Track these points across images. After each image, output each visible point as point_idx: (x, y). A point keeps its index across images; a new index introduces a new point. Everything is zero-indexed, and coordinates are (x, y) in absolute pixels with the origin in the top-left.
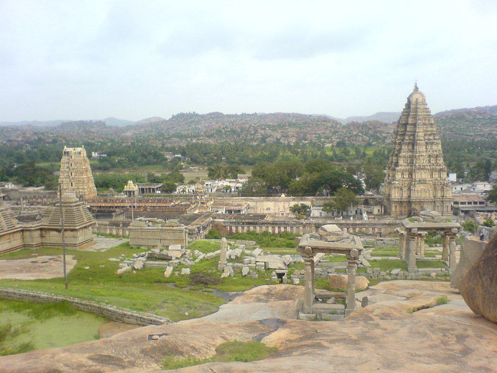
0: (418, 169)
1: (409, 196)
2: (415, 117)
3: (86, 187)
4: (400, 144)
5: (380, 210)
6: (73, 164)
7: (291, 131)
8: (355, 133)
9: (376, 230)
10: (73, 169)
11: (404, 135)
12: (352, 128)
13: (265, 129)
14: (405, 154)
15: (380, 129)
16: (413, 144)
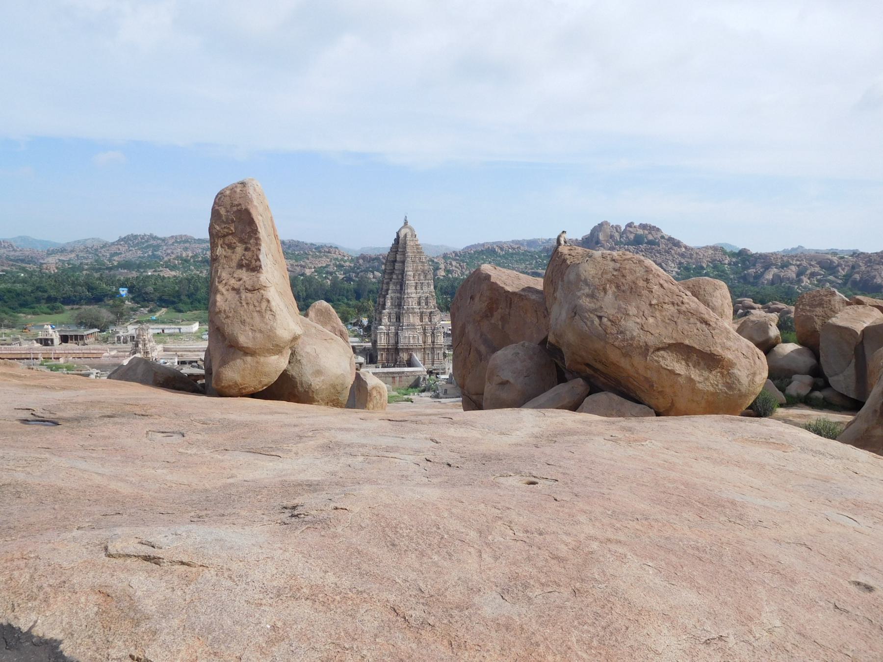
1: (397, 343)
2: (404, 253)
4: (388, 283)
11: (392, 273)
12: (361, 261)
16: (402, 285)
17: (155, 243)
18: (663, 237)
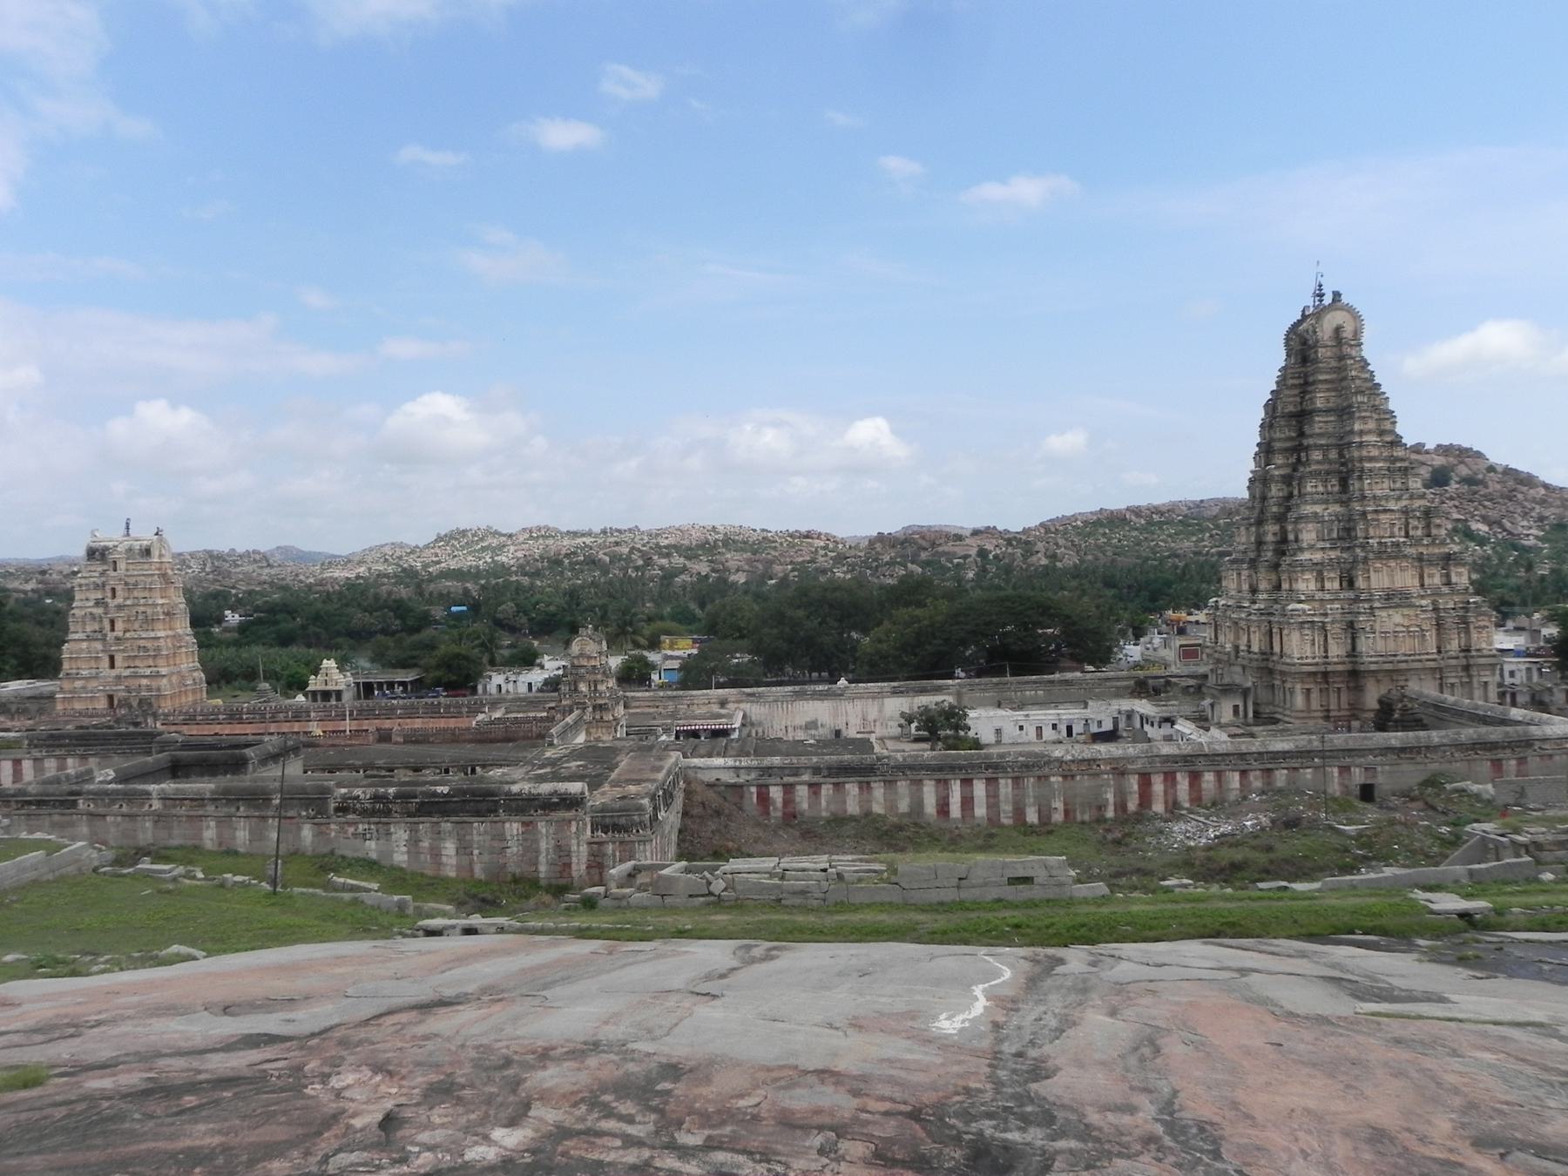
0: (1383, 554)
1: (1353, 652)
3: (164, 671)
5: (1241, 709)
6: (119, 588)
7: (733, 559)
8: (887, 558)
9: (1358, 777)
10: (120, 607)
12: (878, 546)
13: (668, 555)
14: (1318, 509)
15: (945, 548)
17: (495, 542)
18: (1491, 469)
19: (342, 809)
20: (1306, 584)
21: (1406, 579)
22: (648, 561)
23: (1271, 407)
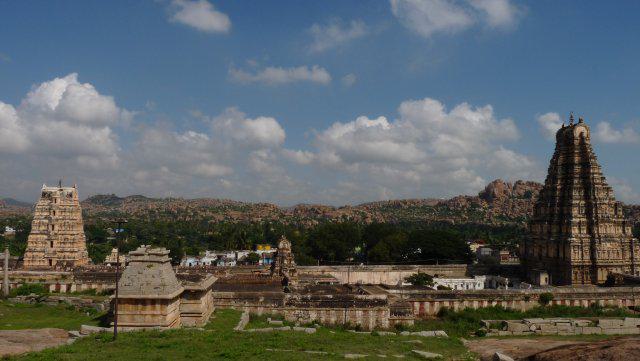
0: (603, 221)
1: (593, 258)
6: (57, 211)
10: (57, 220)
19: (289, 304)
20: (575, 231)
21: (612, 230)
22: (196, 214)
23: (554, 162)
